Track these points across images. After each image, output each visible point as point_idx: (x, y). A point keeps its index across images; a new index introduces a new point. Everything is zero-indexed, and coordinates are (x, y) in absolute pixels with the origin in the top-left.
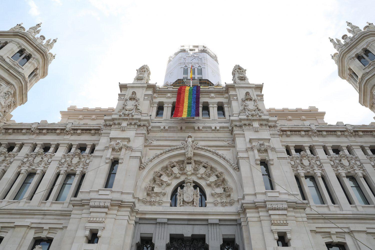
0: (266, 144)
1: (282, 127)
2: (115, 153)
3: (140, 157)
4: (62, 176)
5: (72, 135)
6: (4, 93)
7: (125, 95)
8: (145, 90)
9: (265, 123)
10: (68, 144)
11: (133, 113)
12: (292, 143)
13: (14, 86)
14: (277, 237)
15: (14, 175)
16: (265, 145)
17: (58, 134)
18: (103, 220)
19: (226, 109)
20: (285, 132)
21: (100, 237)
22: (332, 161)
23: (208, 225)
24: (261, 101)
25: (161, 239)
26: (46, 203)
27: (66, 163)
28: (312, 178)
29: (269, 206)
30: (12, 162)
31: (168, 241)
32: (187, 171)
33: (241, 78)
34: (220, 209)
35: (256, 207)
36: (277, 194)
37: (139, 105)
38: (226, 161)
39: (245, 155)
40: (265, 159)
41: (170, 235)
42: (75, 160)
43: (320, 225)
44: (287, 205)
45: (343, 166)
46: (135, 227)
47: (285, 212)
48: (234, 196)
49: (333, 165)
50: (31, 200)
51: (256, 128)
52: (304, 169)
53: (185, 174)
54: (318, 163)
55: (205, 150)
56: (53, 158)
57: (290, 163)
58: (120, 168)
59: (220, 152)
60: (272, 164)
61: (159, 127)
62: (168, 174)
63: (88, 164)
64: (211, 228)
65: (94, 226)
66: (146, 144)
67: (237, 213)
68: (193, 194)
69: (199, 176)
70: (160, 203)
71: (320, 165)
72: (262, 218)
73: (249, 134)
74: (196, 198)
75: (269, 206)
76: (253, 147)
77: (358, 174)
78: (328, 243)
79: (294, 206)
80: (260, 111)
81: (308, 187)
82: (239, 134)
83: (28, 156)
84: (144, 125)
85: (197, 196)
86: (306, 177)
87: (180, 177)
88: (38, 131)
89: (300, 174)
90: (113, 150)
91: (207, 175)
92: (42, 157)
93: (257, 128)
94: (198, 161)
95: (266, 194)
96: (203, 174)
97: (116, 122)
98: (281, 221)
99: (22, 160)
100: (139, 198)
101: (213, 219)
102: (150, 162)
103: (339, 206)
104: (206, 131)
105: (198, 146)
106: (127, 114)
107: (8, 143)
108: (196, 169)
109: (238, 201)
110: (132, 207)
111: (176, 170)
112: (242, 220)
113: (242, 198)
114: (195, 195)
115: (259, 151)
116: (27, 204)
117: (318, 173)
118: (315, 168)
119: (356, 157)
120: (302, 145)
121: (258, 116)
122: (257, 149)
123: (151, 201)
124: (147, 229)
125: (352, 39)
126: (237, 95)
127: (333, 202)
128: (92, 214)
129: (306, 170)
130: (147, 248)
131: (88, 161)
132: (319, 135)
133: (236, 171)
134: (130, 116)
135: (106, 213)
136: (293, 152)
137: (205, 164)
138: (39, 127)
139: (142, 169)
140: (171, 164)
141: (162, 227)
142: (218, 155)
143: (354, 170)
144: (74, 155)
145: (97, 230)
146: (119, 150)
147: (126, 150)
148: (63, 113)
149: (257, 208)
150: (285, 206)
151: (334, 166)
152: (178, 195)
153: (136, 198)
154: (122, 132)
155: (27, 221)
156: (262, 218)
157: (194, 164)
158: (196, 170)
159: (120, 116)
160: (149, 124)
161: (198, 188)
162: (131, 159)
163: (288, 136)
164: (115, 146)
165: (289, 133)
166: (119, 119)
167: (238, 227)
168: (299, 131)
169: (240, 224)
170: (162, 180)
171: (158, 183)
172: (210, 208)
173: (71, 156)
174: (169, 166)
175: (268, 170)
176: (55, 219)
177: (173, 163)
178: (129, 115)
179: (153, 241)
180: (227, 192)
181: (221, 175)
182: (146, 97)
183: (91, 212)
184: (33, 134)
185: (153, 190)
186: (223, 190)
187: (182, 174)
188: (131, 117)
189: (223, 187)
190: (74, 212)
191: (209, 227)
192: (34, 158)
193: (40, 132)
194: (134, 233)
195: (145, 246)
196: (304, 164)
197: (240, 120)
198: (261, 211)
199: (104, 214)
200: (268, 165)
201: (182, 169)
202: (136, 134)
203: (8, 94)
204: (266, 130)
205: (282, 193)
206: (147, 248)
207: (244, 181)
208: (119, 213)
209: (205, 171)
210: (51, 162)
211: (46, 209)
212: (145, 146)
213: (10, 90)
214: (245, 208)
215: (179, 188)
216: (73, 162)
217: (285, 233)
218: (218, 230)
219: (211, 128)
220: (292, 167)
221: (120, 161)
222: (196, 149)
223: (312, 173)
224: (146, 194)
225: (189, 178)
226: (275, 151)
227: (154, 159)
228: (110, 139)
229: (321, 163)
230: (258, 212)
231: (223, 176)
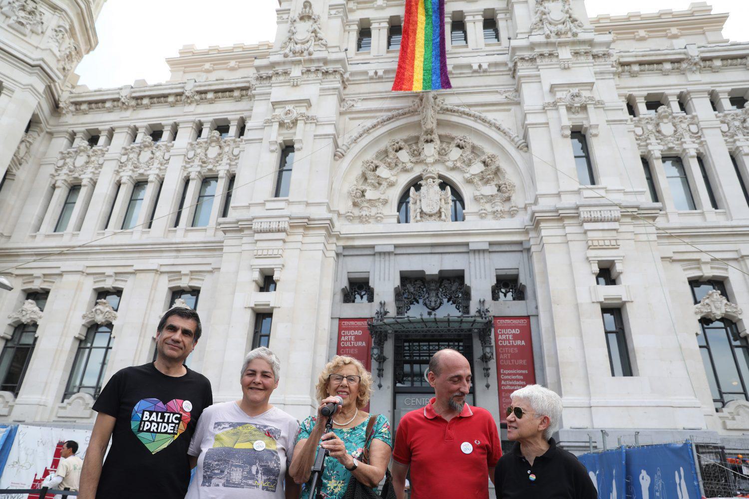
0: (585, 94)
1: (622, 57)
2: (284, 131)
3: (334, 135)
4: (195, 182)
5: (198, 103)
6: (52, 30)
7: (290, 10)
9: (585, 49)
10: (194, 122)
13: (66, 13)
14: (597, 270)
15: (111, 187)
16: (583, 96)
17: (173, 105)
18: (280, 252)
19: (502, 25)
20: (629, 67)
21: (278, 280)
23: (468, 253)
25: (384, 280)
26: (176, 231)
28: (678, 161)
29: (584, 214)
30: (102, 164)
31: (397, 283)
32: (426, 156)
34: (491, 224)
35: (559, 217)
36: (602, 193)
37: (320, 29)
38: (501, 133)
39: (541, 119)
40: (581, 126)
41: (401, 272)
42: (213, 151)
43: (682, 248)
46: (337, 262)
47: (615, 225)
48: (518, 200)
49: (725, 132)
50: (150, 227)
51: (564, 60)
52: (663, 143)
53: (422, 162)
54: (694, 128)
56: (171, 151)
57: (634, 132)
59: (490, 116)
60: (596, 135)
61: (366, 73)
62: (389, 164)
64: (475, 259)
65: (266, 264)
68: (439, 199)
69: (450, 164)
70: (379, 218)
71: (697, 133)
72: (569, 237)
73: (550, 75)
74: (445, 206)
75: (584, 214)
78: (693, 279)
79: (634, 214)
80: (575, 23)
81: (667, 177)
82: (529, 76)
83: (127, 151)
84: (335, 71)
85: (447, 203)
86: (665, 158)
87: (412, 168)
88: (133, 103)
89: (652, 152)
90: (282, 124)
91: (464, 162)
92: (152, 152)
93: (568, 60)
94: (446, 136)
95: (579, 194)
96: (456, 161)
97: (280, 69)
98: (606, 241)
99: (117, 159)
100: (338, 211)
101: (477, 242)
102: (354, 144)
103: (725, 212)
104: (461, 74)
105: (445, 107)
107: (87, 130)
108: (443, 151)
109: (525, 208)
110: (329, 228)
111: (404, 156)
112: (532, 242)
113: (532, 202)
114: (443, 200)
115: (569, 109)
116: (145, 236)
117: (691, 149)
118: (687, 138)
120: (663, 94)
121: (570, 34)
122: (566, 106)
124: (359, 266)
127: (715, 205)
128: (260, 244)
129: (666, 144)
130: (362, 297)
131: (236, 152)
132: (705, 67)
133: (521, 151)
135: (284, 241)
136: (642, 107)
137: (461, 140)
138: (134, 95)
139: (340, 157)
140: (394, 145)
141: (385, 261)
142: (485, 121)
144: (209, 142)
145: (272, 270)
147: (306, 123)
148: (172, 63)
149: (561, 219)
150: (617, 213)
151: (727, 134)
152: (411, 203)
153: (334, 211)
154: (295, 88)
155: (153, 263)
156: (569, 237)
157: (438, 142)
158: (442, 153)
159: (286, 56)
160: (344, 67)
161: (448, 188)
162: (317, 141)
163: (633, 75)
164: (283, 117)
165: (636, 68)
166: (284, 63)
167: (525, 254)
168: (660, 62)
169: (529, 250)
170: (378, 177)
171: (373, 181)
172: (471, 223)
173: (204, 145)
174: (390, 150)
175: (585, 148)
176: (197, 256)
177: (398, 143)
178: (302, 52)
179: (371, 284)
181: (492, 160)
182: (333, 12)
183: (257, 241)
184: (126, 109)
185: (363, 196)
186: (496, 189)
187: (416, 163)
188: (307, 57)
189: (496, 182)
190: (227, 242)
191: (471, 256)
192: (139, 155)
194: (336, 273)
195: (358, 294)
197: (532, 47)
198: (570, 225)
201: (416, 154)
202: (322, 90)
203: (60, 31)
204: (586, 65)
206: (362, 297)
208: (307, 240)
209: (461, 155)
210: (169, 159)
211: (177, 241)
212: (341, 114)
213: (61, 23)
214: (538, 220)
215: (412, 189)
216: (209, 156)
217: (612, 263)
218: (487, 261)
219: (470, 66)
220: (637, 140)
221: (296, 146)
223: (677, 149)
224: (351, 203)
225: (431, 169)
226: (603, 108)
227: (361, 138)
228: (273, 105)
229: (700, 129)
230: (564, 227)
231: (497, 163)
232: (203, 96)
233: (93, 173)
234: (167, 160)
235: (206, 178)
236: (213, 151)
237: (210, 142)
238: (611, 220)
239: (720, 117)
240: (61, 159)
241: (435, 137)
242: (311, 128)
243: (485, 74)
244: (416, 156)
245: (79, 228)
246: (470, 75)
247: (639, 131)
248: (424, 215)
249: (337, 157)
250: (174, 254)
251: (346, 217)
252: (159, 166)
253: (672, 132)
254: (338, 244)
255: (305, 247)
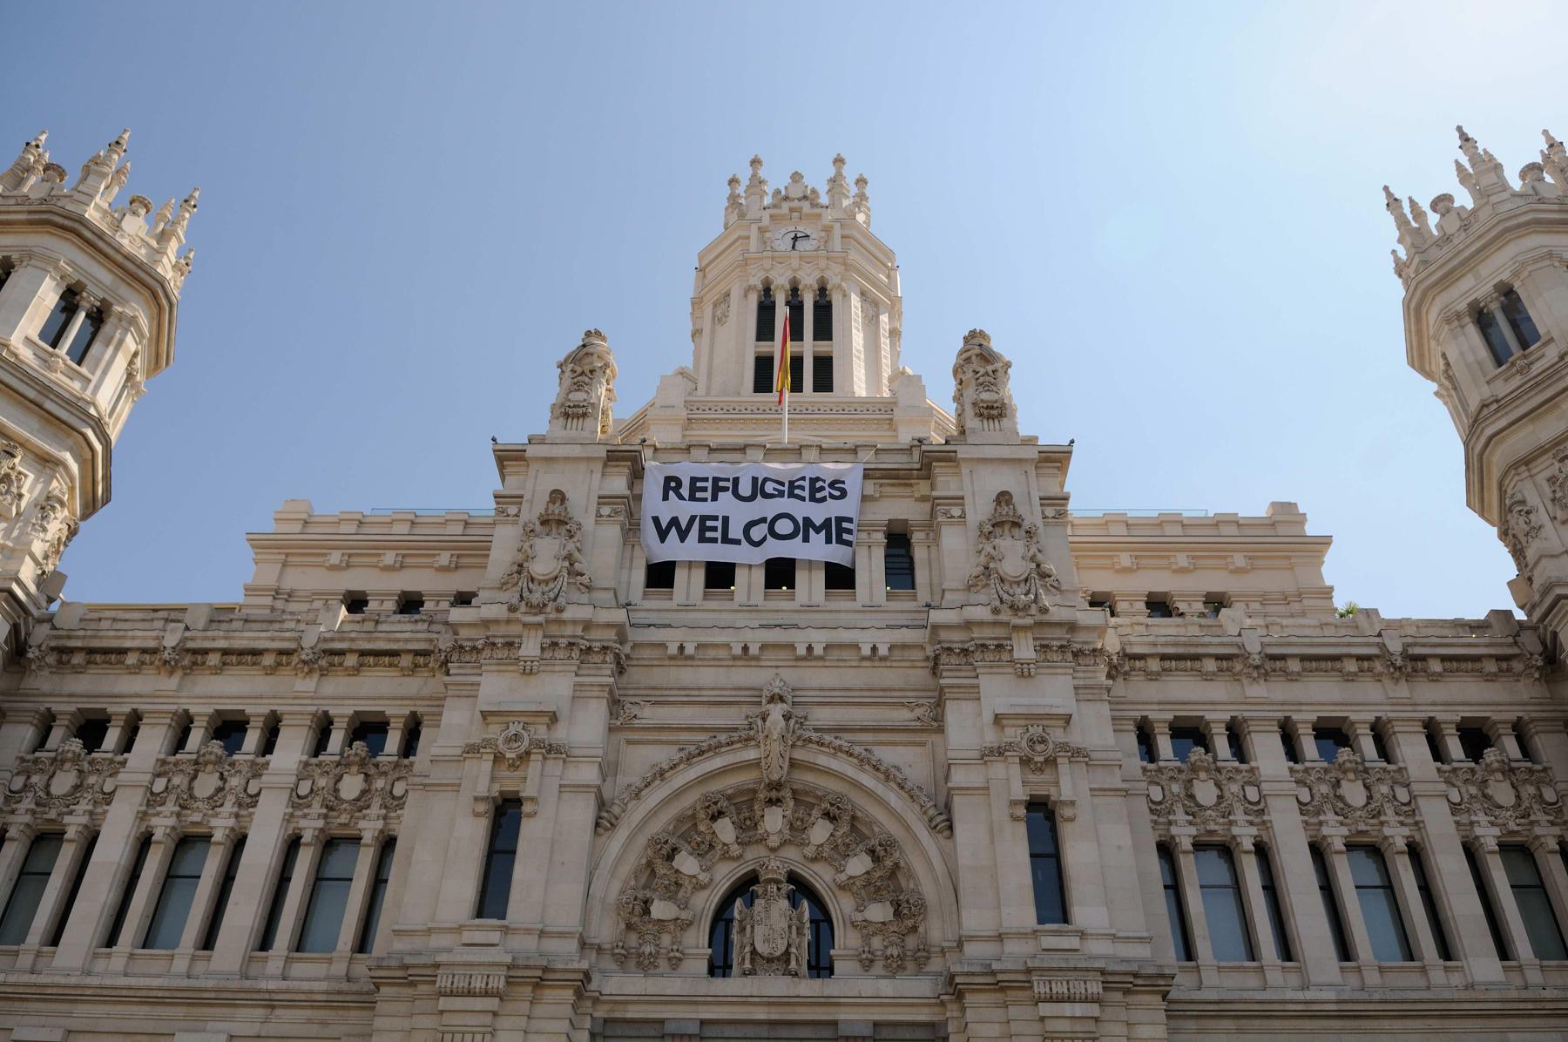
2: (504, 772)
7: (522, 497)
8: (599, 475)
9: (1060, 639)
11: (559, 599)
12: (1162, 707)
15: (128, 848)
17: (272, 670)
19: (919, 554)
20: (1143, 662)
22: (1305, 784)
24: (1056, 525)
27: (317, 798)
29: (1041, 988)
32: (766, 831)
33: (987, 408)
36: (1073, 942)
44: (1103, 982)
45: (1344, 811)
47: (1094, 1010)
49: (1306, 804)
52: (1198, 821)
55: (834, 748)
58: (531, 834)
59: (888, 755)
61: (663, 646)
62: (698, 844)
63: (401, 802)
66: (613, 721)
67: (934, 1001)
69: (810, 851)
71: (1258, 803)
76: (1006, 750)
77: (1391, 840)
80: (1047, 579)
84: (604, 648)
85: (800, 932)
89: (1178, 840)
90: (498, 758)
91: (837, 846)
92: (222, 774)
106: (538, 605)
108: (799, 823)
110: (582, 984)
111: (725, 830)
114: (794, 928)
115: (1025, 762)
118: (1239, 816)
119: (1400, 770)
121: (1034, 608)
122: (1021, 759)
123: (643, 953)
125: (1467, 220)
126: (962, 498)
128: (447, 1019)
132: (1274, 671)
133: (939, 836)
134: (548, 609)
138: (190, 645)
139: (606, 829)
140: (708, 807)
143: (1382, 823)
146: (518, 763)
147: (545, 759)
148: (261, 544)
149: (1000, 987)
150: (1095, 988)
154: (526, 678)
156: (1015, 1028)
157: (792, 803)
158: (797, 829)
160: (622, 640)
168: (1196, 658)
176: (309, 1021)
177: (715, 803)
178: (545, 605)
180: (907, 910)
181: (886, 850)
182: (606, 510)
183: (442, 1012)
185: (647, 912)
186: (892, 910)
188: (553, 616)
192: (195, 777)
193: (195, 663)
196: (1200, 798)
198: (1015, 1003)
199: (488, 1019)
200: (1058, 819)
201: (748, 828)
205: (1092, 935)
207: (966, 881)
208: (539, 1010)
209: (832, 835)
210: (258, 794)
211: (272, 985)
212: (610, 729)
214: (960, 990)
215: (739, 903)
220: (1151, 810)
222: (799, 743)
231: (897, 855)
232: (336, 659)
233: (91, 813)
234: (251, 796)
235: (333, 839)
236: (351, 786)
237: (343, 764)
238: (1086, 1000)
239: (1298, 772)
240: (18, 774)
241: (786, 793)
242: (554, 767)
243: (883, 664)
244: (749, 829)
245: (55, 939)
246: (854, 664)
247: (1156, 793)
248: (758, 958)
249: (600, 830)
250: (260, 1012)
251: (613, 955)
252: (235, 809)
253: (1214, 800)
254: (596, 1014)
255: (535, 1025)
